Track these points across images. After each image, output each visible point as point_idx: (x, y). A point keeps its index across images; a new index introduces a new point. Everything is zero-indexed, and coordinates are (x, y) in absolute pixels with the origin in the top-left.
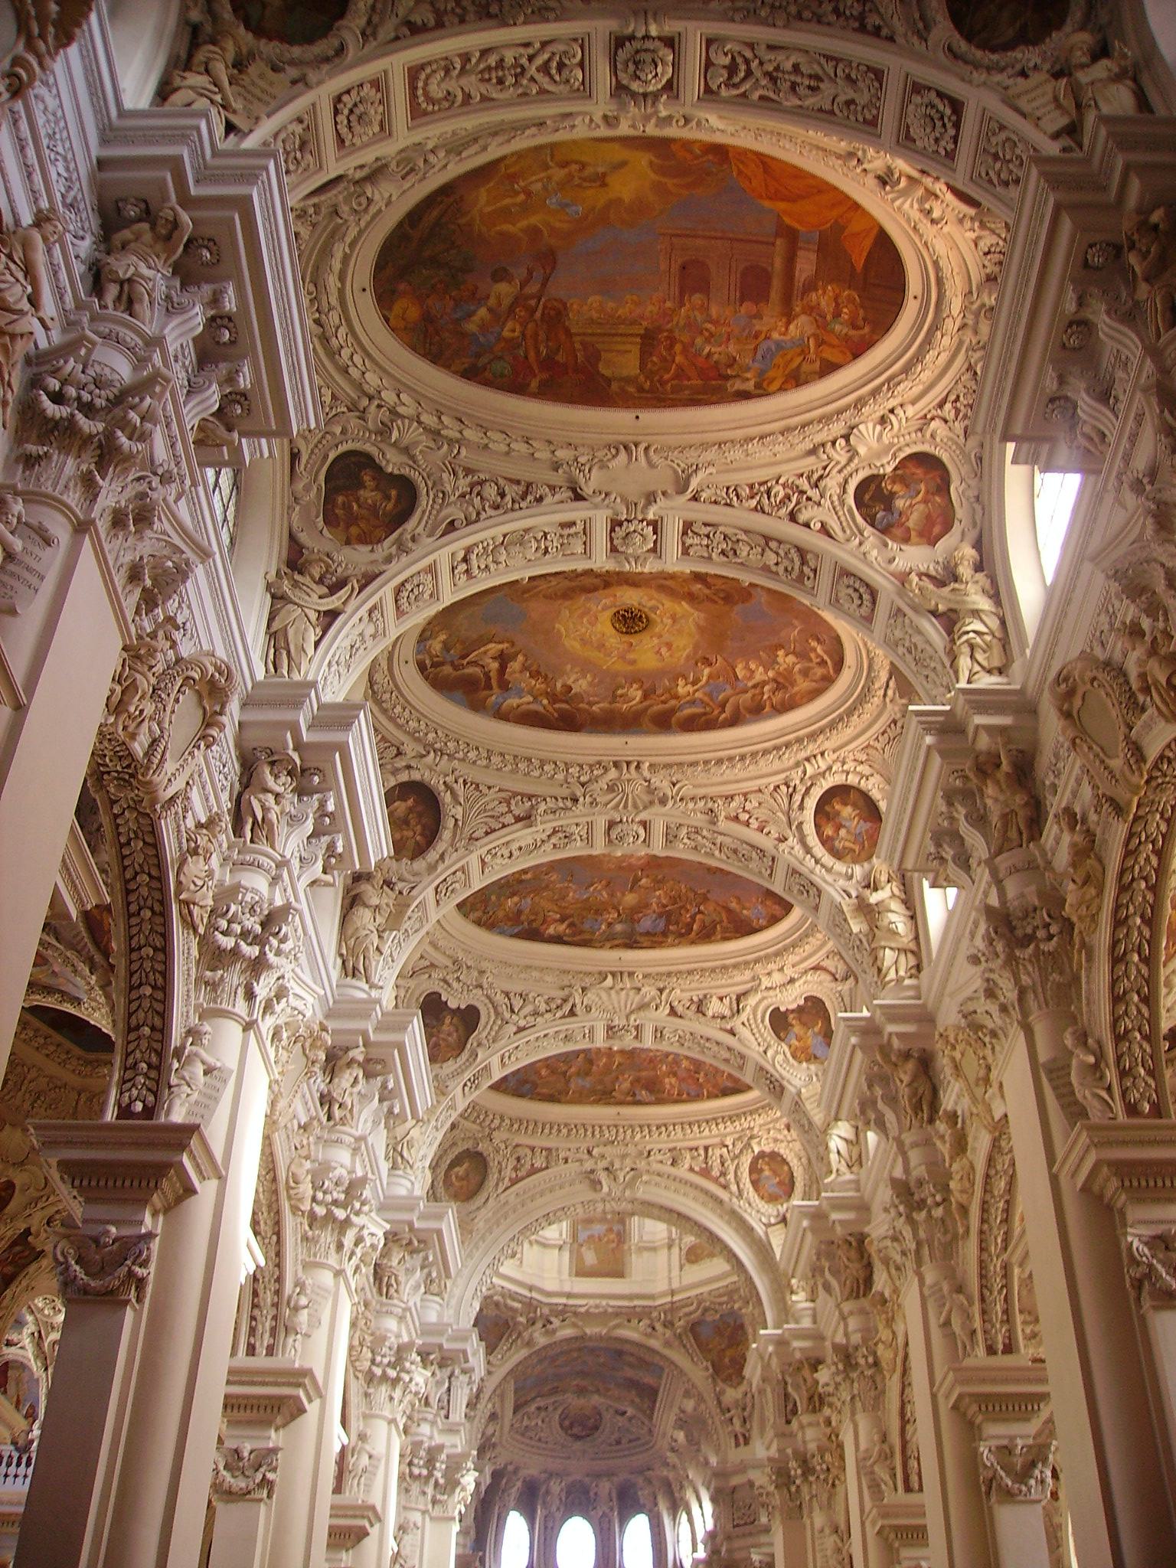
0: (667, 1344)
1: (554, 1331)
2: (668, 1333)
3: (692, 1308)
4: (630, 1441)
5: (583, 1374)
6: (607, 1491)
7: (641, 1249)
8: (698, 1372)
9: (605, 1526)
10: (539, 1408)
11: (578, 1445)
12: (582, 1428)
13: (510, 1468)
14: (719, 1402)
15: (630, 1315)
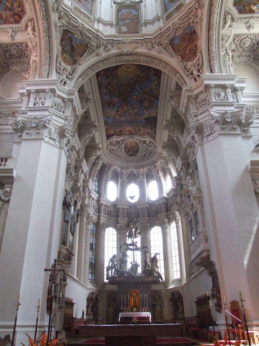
0: (160, 52)
1: (109, 50)
2: (160, 48)
3: (170, 32)
4: (149, 154)
5: (130, 123)
6: (142, 173)
7: (145, 25)
8: (174, 61)
9: (142, 184)
10: (116, 142)
11: (131, 158)
12: (132, 151)
13: (108, 164)
14: (185, 68)
15: (144, 41)
